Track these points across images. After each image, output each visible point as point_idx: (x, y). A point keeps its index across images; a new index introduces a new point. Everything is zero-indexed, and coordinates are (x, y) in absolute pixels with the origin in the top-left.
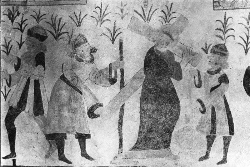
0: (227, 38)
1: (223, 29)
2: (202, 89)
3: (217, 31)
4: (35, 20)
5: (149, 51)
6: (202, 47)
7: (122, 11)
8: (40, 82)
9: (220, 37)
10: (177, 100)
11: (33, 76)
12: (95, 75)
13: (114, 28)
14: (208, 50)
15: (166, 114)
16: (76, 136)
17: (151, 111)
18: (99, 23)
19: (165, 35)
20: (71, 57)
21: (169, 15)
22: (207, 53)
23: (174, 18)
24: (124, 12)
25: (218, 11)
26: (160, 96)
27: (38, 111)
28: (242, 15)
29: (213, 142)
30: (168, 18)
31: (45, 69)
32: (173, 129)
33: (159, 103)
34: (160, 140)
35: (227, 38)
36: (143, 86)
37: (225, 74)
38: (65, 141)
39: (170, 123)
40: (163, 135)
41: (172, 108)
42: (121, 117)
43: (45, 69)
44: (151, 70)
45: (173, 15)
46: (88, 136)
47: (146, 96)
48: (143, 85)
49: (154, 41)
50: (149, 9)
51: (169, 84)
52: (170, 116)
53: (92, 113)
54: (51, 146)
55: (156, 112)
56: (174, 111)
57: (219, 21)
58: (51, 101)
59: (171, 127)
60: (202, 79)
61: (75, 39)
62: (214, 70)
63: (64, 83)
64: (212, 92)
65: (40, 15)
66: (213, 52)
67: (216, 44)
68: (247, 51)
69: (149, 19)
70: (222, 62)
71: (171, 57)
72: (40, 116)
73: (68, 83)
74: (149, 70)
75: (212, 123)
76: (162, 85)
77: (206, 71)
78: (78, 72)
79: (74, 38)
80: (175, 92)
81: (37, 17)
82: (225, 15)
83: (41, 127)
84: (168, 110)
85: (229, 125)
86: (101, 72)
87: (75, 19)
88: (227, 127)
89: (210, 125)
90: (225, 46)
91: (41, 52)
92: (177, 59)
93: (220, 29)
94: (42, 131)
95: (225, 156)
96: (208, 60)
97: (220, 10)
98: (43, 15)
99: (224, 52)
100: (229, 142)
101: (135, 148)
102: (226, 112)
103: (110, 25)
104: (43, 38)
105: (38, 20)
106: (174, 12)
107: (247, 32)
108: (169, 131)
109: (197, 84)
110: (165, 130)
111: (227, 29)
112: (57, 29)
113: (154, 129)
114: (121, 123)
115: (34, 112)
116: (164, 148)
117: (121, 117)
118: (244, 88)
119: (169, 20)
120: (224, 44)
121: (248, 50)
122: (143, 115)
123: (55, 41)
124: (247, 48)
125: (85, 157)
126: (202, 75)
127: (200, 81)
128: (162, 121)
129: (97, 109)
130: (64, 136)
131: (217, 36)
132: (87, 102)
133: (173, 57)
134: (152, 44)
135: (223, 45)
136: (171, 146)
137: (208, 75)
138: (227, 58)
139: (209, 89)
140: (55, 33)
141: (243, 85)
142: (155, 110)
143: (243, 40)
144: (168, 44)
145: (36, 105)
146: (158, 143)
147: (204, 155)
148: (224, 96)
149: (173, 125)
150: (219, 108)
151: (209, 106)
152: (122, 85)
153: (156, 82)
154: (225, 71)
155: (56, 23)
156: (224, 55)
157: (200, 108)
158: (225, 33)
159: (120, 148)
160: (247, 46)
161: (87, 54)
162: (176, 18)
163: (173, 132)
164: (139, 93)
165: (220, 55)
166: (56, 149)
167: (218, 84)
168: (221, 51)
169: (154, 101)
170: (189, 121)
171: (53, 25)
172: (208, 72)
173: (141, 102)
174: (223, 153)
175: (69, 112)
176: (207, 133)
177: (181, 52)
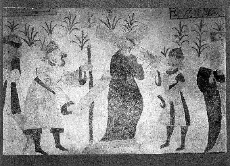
0: (182, 43)
1: (178, 35)
2: (162, 87)
4: (10, 30)
5: (114, 56)
6: (161, 51)
7: (89, 20)
8: (16, 84)
11: (10, 78)
12: (66, 77)
13: (83, 35)
14: (166, 53)
15: (131, 109)
16: (50, 130)
17: (118, 107)
18: (69, 32)
19: (128, 41)
20: (44, 61)
22: (165, 56)
23: (136, 26)
24: (91, 22)
25: (174, 20)
26: (125, 93)
27: (15, 109)
28: (195, 23)
31: (20, 73)
32: (138, 122)
34: (126, 132)
35: (182, 43)
36: (110, 86)
37: (181, 74)
38: (41, 135)
40: (128, 127)
42: (91, 113)
43: (20, 73)
44: (117, 71)
46: (62, 130)
47: (113, 94)
48: (110, 84)
49: (118, 47)
50: (113, 18)
51: (133, 83)
53: (64, 110)
54: (28, 140)
55: (122, 108)
56: (138, 106)
57: (175, 28)
58: (27, 100)
59: (136, 120)
60: (162, 78)
61: (47, 46)
62: (172, 71)
63: (38, 84)
65: (15, 25)
66: (171, 55)
67: (173, 48)
68: (200, 54)
69: (113, 27)
70: (179, 64)
72: (17, 114)
73: (42, 84)
74: (114, 71)
75: (171, 115)
77: (165, 72)
78: (51, 75)
79: (46, 44)
80: (139, 90)
81: (12, 27)
83: (19, 123)
86: (72, 74)
87: (46, 28)
88: (184, 119)
89: (170, 117)
91: (16, 58)
92: (140, 62)
94: (20, 127)
97: (176, 19)
98: (17, 25)
99: (180, 55)
100: (186, 131)
101: (105, 139)
102: (183, 107)
103: (79, 33)
104: (17, 45)
105: (13, 29)
106: (136, 21)
108: (134, 125)
109: (157, 83)
111: (182, 36)
112: (30, 37)
113: (121, 122)
114: (91, 119)
115: (11, 111)
116: (130, 138)
117: (91, 113)
119: (131, 28)
121: (201, 53)
122: (111, 111)
123: (29, 48)
124: (199, 51)
125: (60, 149)
127: (160, 80)
129: (69, 107)
130: (40, 131)
131: (173, 41)
132: (61, 101)
133: (136, 60)
134: (117, 49)
136: (136, 136)
138: (183, 60)
139: (168, 87)
140: (28, 41)
143: (197, 44)
144: (131, 49)
145: (14, 105)
146: (124, 134)
147: (165, 143)
148: (181, 92)
149: (137, 118)
150: (178, 104)
151: (169, 102)
152: (91, 85)
153: (121, 82)
155: (29, 32)
157: (160, 104)
158: (181, 39)
159: (90, 139)
160: (199, 50)
161: (59, 59)
162: (137, 26)
163: (137, 125)
164: (107, 92)
165: (176, 58)
166: (32, 142)
167: (175, 82)
168: (177, 54)
169: (120, 98)
170: (151, 114)
171: (27, 34)
172: (166, 72)
173: (109, 99)
174: (181, 141)
175: (44, 110)
177: (143, 56)
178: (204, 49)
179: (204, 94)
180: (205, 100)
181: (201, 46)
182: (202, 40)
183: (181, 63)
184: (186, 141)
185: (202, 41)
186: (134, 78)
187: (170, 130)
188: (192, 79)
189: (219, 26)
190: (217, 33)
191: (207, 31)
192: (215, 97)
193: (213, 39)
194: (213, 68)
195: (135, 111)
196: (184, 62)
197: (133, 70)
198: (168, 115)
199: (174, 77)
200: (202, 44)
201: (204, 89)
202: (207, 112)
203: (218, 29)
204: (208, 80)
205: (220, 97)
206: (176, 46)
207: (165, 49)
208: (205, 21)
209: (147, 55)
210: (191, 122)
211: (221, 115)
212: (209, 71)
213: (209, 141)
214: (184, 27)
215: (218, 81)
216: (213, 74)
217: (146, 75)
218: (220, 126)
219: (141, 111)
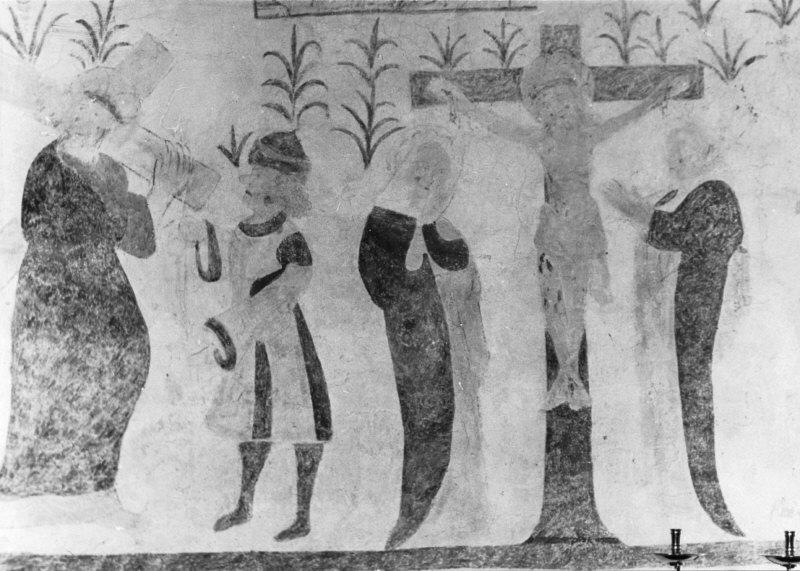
1: (286, 80)
2: (223, 284)
3: (268, 87)
5: (40, 159)
6: (219, 142)
9: (281, 109)
10: (138, 325)
15: (101, 372)
17: (49, 364)
19: (92, 105)
21: (104, 36)
22: (236, 164)
23: (123, 44)
25: (272, 21)
26: (79, 310)
28: (349, 34)
29: (261, 465)
30: (101, 43)
32: (127, 424)
33: (76, 338)
34: (83, 462)
35: (301, 112)
36: (20, 278)
37: (298, 234)
39: (116, 403)
40: (90, 444)
41: (122, 354)
44: (49, 222)
45: (119, 36)
47: (33, 314)
51: (111, 270)
52: (114, 379)
55: (65, 367)
56: (129, 362)
57: (275, 54)
59: (120, 417)
60: (224, 251)
62: (263, 221)
64: (257, 296)
66: (257, 159)
67: (267, 134)
68: (370, 157)
69: (35, 50)
70: (289, 194)
71: (115, 177)
74: (38, 222)
75: (257, 399)
76: (85, 275)
77: (234, 226)
80: (133, 298)
82: (294, 34)
84: (107, 358)
85: (315, 407)
88: (306, 416)
89: (253, 407)
90: (296, 138)
92: (136, 186)
93: (278, 83)
95: (303, 513)
96: (243, 188)
97: (277, 16)
99: (293, 160)
100: (315, 464)
106: (122, 26)
107: (366, 90)
109: (205, 268)
110: (98, 428)
111: (301, 84)
113: (59, 425)
116: (97, 490)
118: (361, 281)
119: (105, 51)
120: (294, 132)
121: (373, 151)
122: (22, 378)
127: (216, 260)
128: (86, 396)
131: (268, 106)
133: (124, 178)
135: (290, 138)
136: (120, 480)
137: (242, 236)
138: (304, 180)
139: (248, 287)
141: (357, 270)
142: (64, 360)
143: (357, 118)
144: (103, 133)
146: (73, 473)
147: (233, 508)
148: (297, 307)
149: (125, 410)
150: (282, 352)
153: (65, 264)
154: (297, 224)
156: (295, 168)
157: (216, 352)
158: (297, 95)
160: (368, 139)
162: (127, 44)
164: (8, 304)
165: (281, 170)
167: (278, 267)
168: (281, 155)
169: (60, 328)
170: (180, 395)
172: (242, 226)
174: (294, 499)
177: (149, 160)
178: (384, 137)
180: (392, 340)
181: (373, 125)
182: (378, 100)
183: (298, 192)
184: (314, 502)
185: (379, 105)
186: (116, 248)
188: (336, 252)
189: (444, 47)
190: (436, 75)
191: (397, 66)
192: (429, 327)
193: (421, 100)
195: (119, 381)
196: (312, 186)
197: (110, 219)
198: (245, 396)
199: (271, 243)
200: (376, 121)
201: (388, 297)
203: (442, 61)
204: (403, 258)
205: (446, 328)
206: (280, 124)
208: (389, 27)
209: (166, 160)
210: (335, 426)
211: (451, 400)
212: (407, 222)
214: (309, 48)
215: (442, 265)
216: (422, 237)
217: (161, 237)
218: (448, 444)
219: (139, 380)
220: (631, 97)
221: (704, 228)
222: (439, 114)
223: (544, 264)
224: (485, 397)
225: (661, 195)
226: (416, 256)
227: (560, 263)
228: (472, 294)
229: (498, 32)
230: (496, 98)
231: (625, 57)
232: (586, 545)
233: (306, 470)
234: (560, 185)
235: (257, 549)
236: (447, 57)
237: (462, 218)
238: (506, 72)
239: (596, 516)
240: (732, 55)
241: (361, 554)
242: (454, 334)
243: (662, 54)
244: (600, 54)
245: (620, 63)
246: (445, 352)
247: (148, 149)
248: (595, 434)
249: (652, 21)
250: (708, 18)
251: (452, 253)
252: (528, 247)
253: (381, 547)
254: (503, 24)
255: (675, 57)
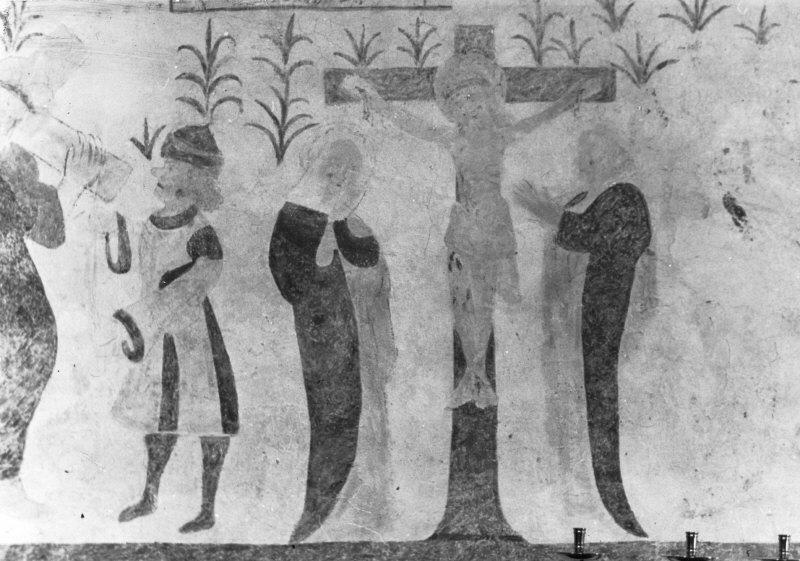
0: (215, 106)
1: (201, 74)
2: (133, 275)
3: (181, 81)
6: (132, 135)
9: (194, 103)
10: (46, 315)
14: (151, 146)
21: (18, 26)
22: (149, 157)
29: (167, 457)
30: (14, 31)
32: (32, 414)
35: (215, 106)
37: (210, 228)
41: (30, 343)
45: (32, 28)
51: (20, 260)
52: (21, 369)
56: (36, 352)
59: (26, 406)
60: (134, 244)
62: (174, 214)
64: (167, 289)
66: (169, 152)
67: (180, 127)
68: (283, 152)
71: (26, 166)
75: (164, 391)
77: (145, 218)
80: (41, 289)
82: (209, 28)
84: (14, 347)
85: (223, 400)
88: (213, 408)
89: (159, 400)
90: (209, 132)
92: (47, 176)
93: (192, 77)
95: (208, 505)
96: (155, 180)
99: (206, 154)
102: (210, 357)
107: (280, 86)
109: (115, 260)
111: (215, 78)
118: (271, 276)
120: (207, 126)
121: (286, 148)
126: (134, 228)
131: (182, 99)
133: (34, 168)
135: (204, 131)
136: (25, 468)
137: (152, 229)
138: (216, 174)
139: (158, 278)
141: (267, 266)
147: (138, 499)
149: (31, 400)
150: (190, 343)
151: (157, 337)
156: (208, 162)
158: (211, 89)
160: (282, 134)
165: (193, 164)
167: (188, 260)
168: (194, 148)
170: (86, 386)
172: (153, 219)
174: (199, 493)
176: (148, 426)
177: (62, 153)
178: (297, 133)
179: (295, 310)
180: (301, 335)
181: (287, 121)
182: (290, 98)
183: (209, 185)
184: (219, 495)
185: (293, 101)
186: (25, 237)
187: (159, 450)
188: (247, 243)
189: (358, 44)
191: (311, 63)
192: (339, 323)
193: (334, 96)
194: (332, 212)
195: (26, 371)
196: (224, 181)
197: (19, 208)
198: (151, 388)
200: (290, 116)
201: (297, 292)
202: (306, 380)
203: (356, 58)
204: (313, 255)
206: (193, 118)
207: (146, 128)
208: (305, 23)
209: (78, 149)
210: (242, 421)
212: (319, 219)
213: (308, 500)
215: (352, 262)
216: (333, 233)
218: (354, 439)
219: (46, 371)
220: (543, 99)
221: (612, 230)
222: (354, 110)
223: (453, 263)
224: (393, 393)
225: (571, 197)
226: (326, 252)
227: (471, 266)
228: (381, 294)
229: (411, 31)
230: (409, 97)
231: (539, 59)
232: (489, 543)
233: (212, 464)
234: (473, 184)
235: (162, 540)
236: (362, 53)
237: (373, 215)
238: (419, 71)
239: (500, 514)
240: (645, 58)
241: (266, 547)
242: (363, 331)
243: (575, 56)
244: (512, 55)
245: (533, 64)
246: (354, 350)
247: (61, 140)
248: (501, 432)
249: (564, 24)
250: (622, 21)
251: (362, 249)
252: (437, 245)
253: (285, 540)
254: (418, 23)
255: (589, 58)
